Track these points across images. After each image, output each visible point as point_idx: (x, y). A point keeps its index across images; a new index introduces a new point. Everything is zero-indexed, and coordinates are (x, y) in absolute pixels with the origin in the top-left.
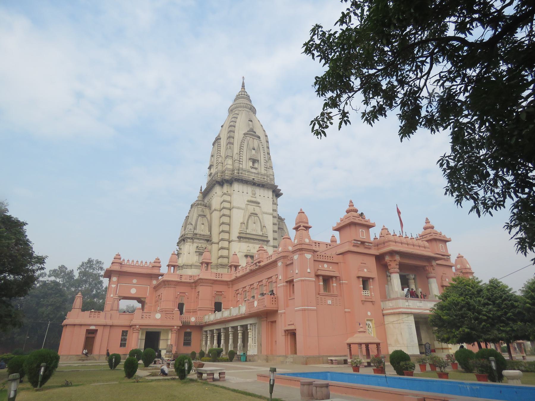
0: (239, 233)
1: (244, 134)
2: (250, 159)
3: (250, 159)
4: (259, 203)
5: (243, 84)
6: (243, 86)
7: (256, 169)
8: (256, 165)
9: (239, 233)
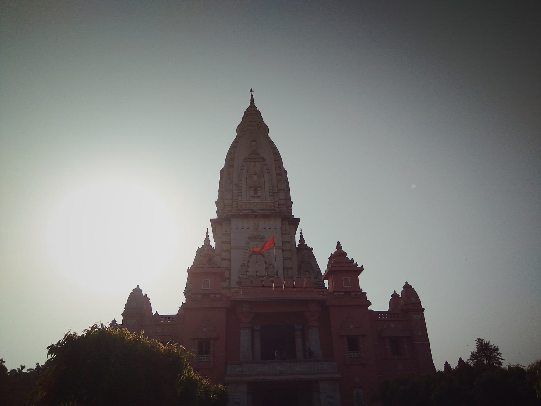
0: (239, 278)
1: (244, 159)
2: (250, 187)
3: (250, 187)
4: (263, 237)
5: (252, 97)
6: (252, 100)
7: (259, 197)
8: (259, 193)
9: (239, 278)
